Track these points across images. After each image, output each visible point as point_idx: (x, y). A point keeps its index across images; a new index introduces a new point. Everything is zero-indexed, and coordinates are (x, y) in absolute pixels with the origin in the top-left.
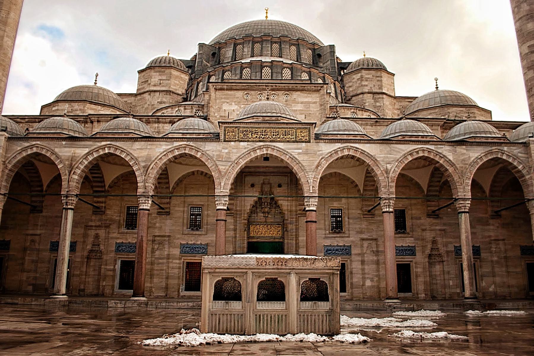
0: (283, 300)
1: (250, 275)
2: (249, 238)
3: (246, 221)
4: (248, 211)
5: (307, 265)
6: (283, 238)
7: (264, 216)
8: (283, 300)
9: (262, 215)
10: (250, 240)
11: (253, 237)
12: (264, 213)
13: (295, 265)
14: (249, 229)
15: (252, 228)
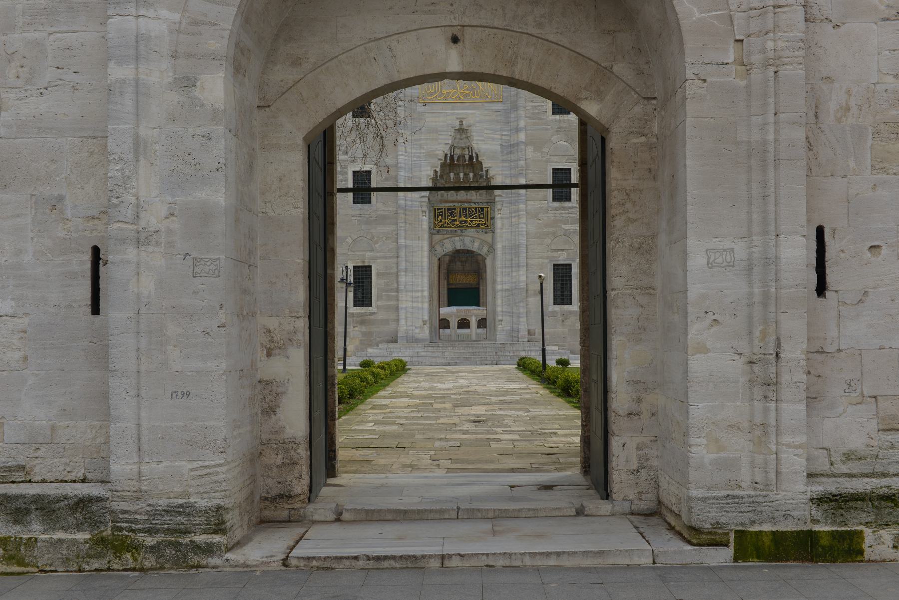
0: (469, 328)
1: (454, 317)
2: (448, 284)
3: (446, 271)
4: (448, 262)
5: (479, 312)
6: (479, 284)
7: (461, 265)
8: (469, 328)
9: (460, 264)
10: (450, 287)
11: (452, 284)
12: (462, 262)
13: (475, 312)
14: (448, 277)
15: (451, 276)
